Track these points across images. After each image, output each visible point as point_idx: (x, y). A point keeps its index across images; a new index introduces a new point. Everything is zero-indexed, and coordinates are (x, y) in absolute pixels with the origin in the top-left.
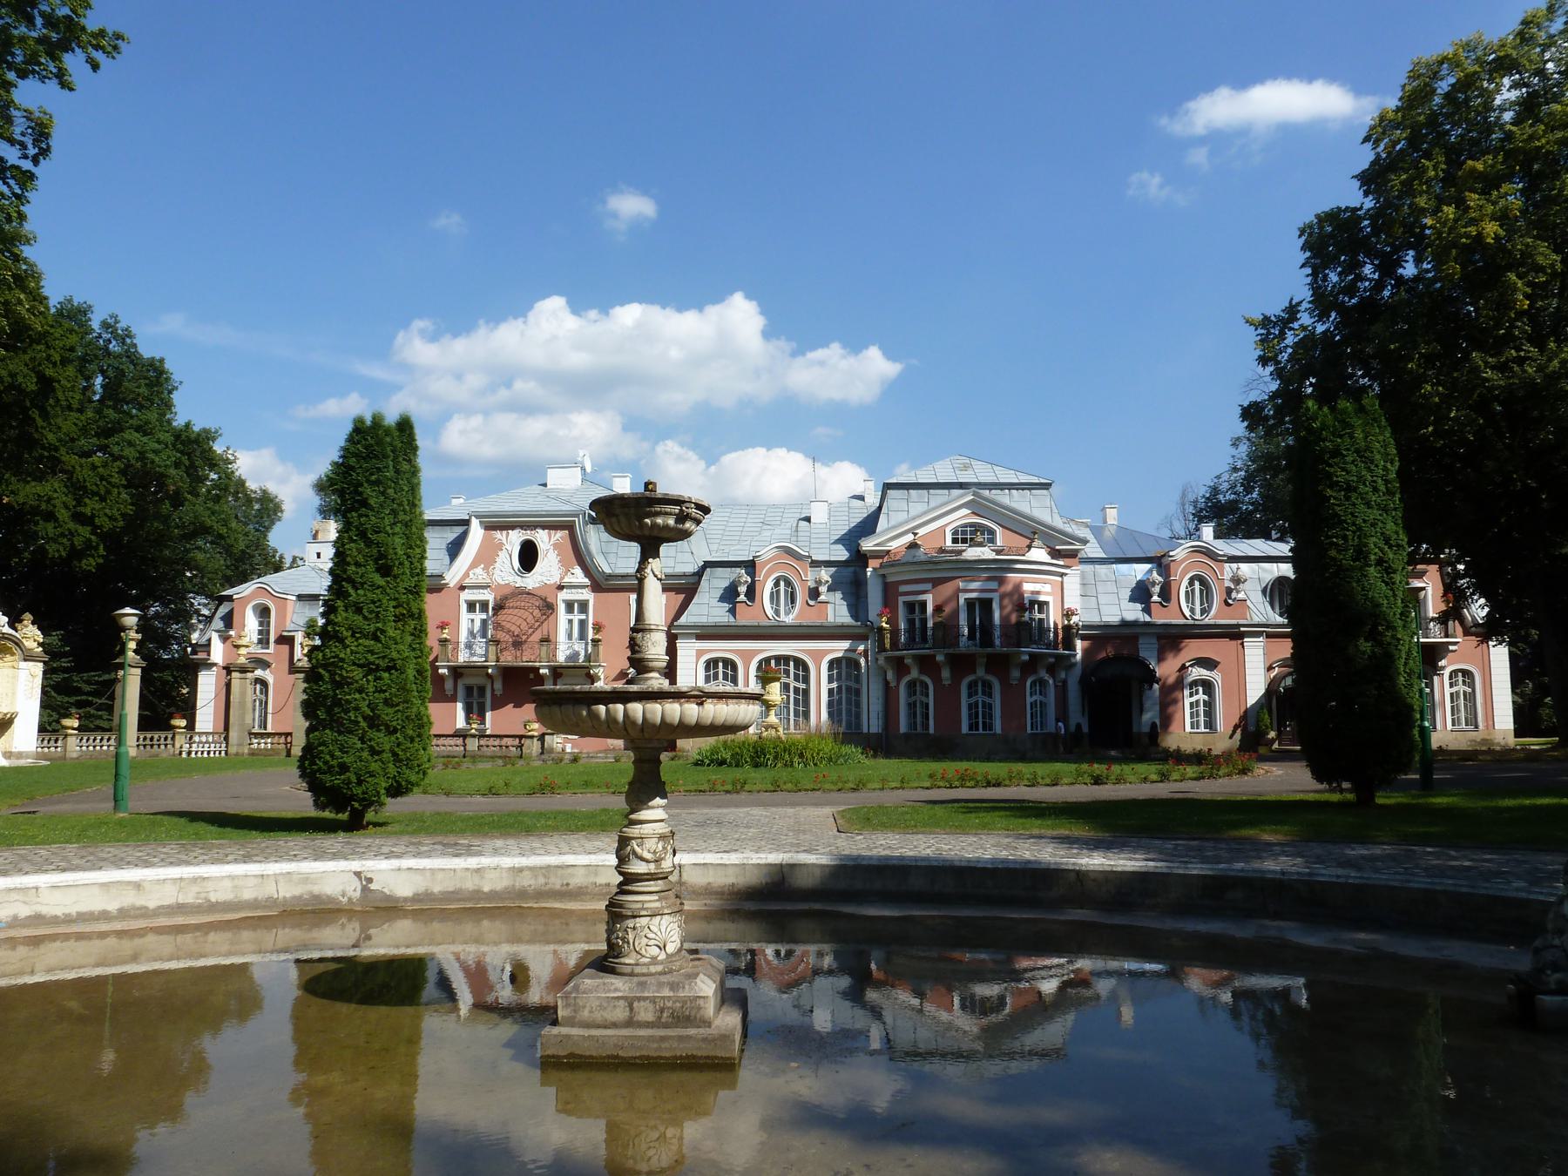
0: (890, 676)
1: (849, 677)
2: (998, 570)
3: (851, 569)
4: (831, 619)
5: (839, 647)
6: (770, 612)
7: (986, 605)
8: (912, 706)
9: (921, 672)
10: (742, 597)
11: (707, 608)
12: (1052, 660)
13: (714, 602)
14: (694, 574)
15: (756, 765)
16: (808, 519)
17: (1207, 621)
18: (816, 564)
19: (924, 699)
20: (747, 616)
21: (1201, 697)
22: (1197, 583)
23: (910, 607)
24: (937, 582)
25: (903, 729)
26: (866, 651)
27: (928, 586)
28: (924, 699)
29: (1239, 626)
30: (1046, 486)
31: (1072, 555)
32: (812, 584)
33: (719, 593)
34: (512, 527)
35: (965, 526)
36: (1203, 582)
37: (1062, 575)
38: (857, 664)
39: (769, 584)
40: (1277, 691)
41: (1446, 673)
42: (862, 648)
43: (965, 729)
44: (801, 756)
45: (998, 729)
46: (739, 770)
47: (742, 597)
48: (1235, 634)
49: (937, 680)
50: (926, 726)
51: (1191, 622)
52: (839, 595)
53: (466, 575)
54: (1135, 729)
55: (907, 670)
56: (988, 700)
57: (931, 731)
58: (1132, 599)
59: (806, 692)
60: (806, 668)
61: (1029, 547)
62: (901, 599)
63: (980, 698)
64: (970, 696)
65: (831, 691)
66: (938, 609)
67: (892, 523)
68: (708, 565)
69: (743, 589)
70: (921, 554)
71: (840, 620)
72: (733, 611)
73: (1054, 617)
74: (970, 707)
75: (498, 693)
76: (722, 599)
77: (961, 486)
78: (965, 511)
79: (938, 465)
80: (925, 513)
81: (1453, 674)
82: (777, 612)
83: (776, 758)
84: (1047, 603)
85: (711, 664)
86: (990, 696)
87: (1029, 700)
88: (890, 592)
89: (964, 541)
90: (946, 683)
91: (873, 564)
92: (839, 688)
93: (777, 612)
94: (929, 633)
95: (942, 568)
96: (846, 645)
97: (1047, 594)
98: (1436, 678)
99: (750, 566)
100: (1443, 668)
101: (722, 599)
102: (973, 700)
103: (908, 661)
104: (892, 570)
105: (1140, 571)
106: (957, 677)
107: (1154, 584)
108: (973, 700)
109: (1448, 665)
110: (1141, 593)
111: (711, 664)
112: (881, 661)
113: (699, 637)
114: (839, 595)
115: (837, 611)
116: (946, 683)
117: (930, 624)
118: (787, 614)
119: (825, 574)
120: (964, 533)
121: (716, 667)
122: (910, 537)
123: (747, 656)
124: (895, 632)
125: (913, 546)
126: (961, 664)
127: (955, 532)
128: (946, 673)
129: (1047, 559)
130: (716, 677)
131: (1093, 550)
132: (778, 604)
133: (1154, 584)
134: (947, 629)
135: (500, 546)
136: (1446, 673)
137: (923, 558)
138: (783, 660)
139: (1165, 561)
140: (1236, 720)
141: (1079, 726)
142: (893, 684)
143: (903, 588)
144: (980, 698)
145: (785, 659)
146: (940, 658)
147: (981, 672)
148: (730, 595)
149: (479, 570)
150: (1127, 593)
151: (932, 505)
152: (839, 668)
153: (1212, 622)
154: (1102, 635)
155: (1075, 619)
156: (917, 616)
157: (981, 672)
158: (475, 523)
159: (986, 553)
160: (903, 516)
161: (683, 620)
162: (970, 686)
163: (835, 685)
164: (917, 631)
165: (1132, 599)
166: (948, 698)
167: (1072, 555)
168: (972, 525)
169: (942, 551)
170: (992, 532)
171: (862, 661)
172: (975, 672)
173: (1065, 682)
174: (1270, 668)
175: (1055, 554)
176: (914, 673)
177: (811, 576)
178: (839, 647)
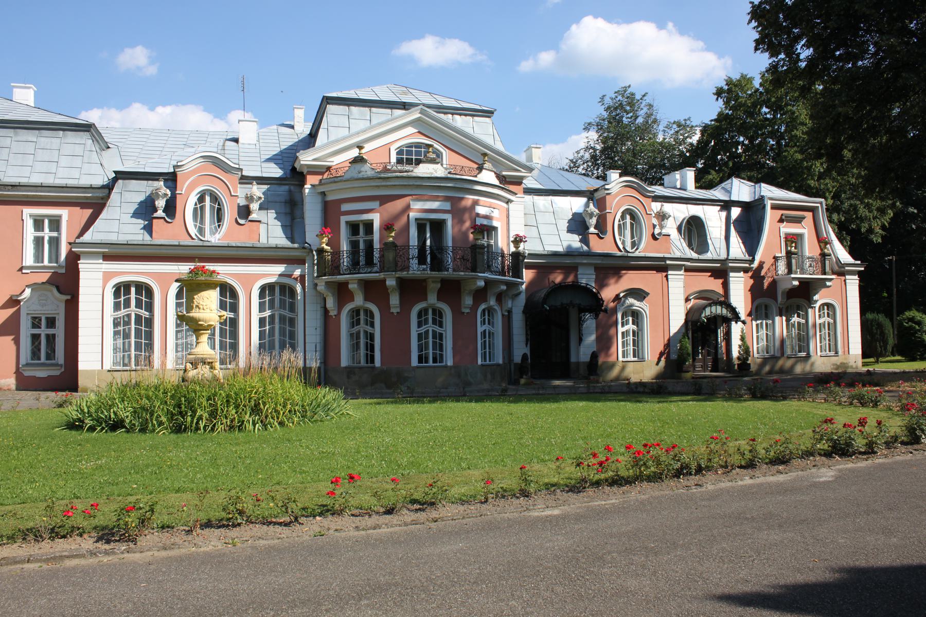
0: (331, 303)
1: (282, 303)
2: (456, 189)
3: (287, 188)
4: (263, 241)
5: (272, 272)
6: (193, 231)
7: (438, 227)
8: (355, 337)
9: (366, 299)
10: (160, 213)
11: (118, 223)
12: (504, 287)
13: (127, 218)
14: (103, 187)
15: (179, 429)
16: (236, 140)
17: (637, 254)
18: (246, 180)
19: (369, 329)
20: (166, 234)
21: (631, 327)
22: (628, 217)
23: (354, 228)
24: (384, 200)
25: (344, 363)
26: (302, 278)
27: (375, 205)
28: (369, 329)
29: (664, 259)
30: (488, 113)
31: (518, 181)
32: (242, 202)
33: (133, 208)
35: (410, 146)
36: (633, 217)
37: (508, 201)
38: (292, 292)
39: (193, 199)
40: (699, 320)
41: (817, 305)
42: (297, 272)
44: (256, 410)
45: (450, 363)
46: (142, 437)
47: (160, 213)
48: (661, 266)
49: (384, 306)
50: (371, 359)
51: (623, 253)
52: (272, 214)
54: (573, 359)
55: (350, 297)
56: (438, 329)
57: (378, 363)
58: (570, 230)
60: (234, 294)
61: (480, 168)
62: (344, 219)
63: (430, 327)
64: (420, 325)
65: (262, 322)
66: (387, 227)
67: (332, 138)
68: (120, 175)
69: (161, 203)
70: (367, 170)
71: (273, 242)
72: (149, 229)
73: (503, 243)
74: (420, 336)
76: (136, 215)
77: (405, 106)
78: (411, 130)
79: (376, 89)
80: (364, 131)
81: (823, 305)
82: (201, 231)
83: (213, 414)
84: (495, 229)
85: (122, 289)
87: (480, 329)
88: (330, 212)
89: (409, 162)
90: (395, 310)
91: (312, 180)
92: (272, 317)
93: (201, 231)
94: (376, 254)
95: (389, 186)
96: (280, 269)
97: (498, 220)
98: (810, 310)
99: (171, 179)
100: (816, 301)
101: (136, 215)
102: (423, 329)
103: (352, 286)
104: (334, 187)
105: (578, 204)
106: (406, 304)
107: (591, 215)
108: (423, 329)
109: (820, 298)
110: (578, 224)
111: (122, 289)
112: (321, 287)
113: (107, 257)
114: (272, 214)
115: (270, 231)
116: (393, 310)
117: (377, 245)
118: (213, 233)
119: (258, 191)
120: (409, 153)
121: (127, 292)
122: (355, 153)
124: (336, 253)
125: (359, 160)
126: (412, 289)
127: (400, 152)
128: (394, 300)
129: (497, 182)
130: (127, 304)
131: (530, 183)
132: (202, 221)
133: (591, 215)
134: (395, 253)
136: (817, 305)
137: (370, 173)
139: (597, 195)
140: (661, 348)
141: (524, 356)
142: (333, 313)
143: (345, 207)
146: (391, 282)
147: (432, 299)
148: (146, 210)
150: (564, 225)
151: (374, 122)
152: (272, 292)
153: (642, 254)
154: (549, 263)
155: (522, 246)
156: (361, 238)
157: (432, 299)
159: (437, 170)
160: (345, 132)
161: (87, 237)
162: (419, 315)
163: (267, 313)
164: (362, 255)
165: (570, 230)
166: (396, 329)
167: (518, 181)
168: (418, 145)
169: (386, 170)
170: (439, 155)
171: (299, 288)
172: (426, 299)
173: (510, 312)
174: (687, 300)
175: (502, 179)
176: (359, 300)
177: (241, 192)
178: (272, 272)
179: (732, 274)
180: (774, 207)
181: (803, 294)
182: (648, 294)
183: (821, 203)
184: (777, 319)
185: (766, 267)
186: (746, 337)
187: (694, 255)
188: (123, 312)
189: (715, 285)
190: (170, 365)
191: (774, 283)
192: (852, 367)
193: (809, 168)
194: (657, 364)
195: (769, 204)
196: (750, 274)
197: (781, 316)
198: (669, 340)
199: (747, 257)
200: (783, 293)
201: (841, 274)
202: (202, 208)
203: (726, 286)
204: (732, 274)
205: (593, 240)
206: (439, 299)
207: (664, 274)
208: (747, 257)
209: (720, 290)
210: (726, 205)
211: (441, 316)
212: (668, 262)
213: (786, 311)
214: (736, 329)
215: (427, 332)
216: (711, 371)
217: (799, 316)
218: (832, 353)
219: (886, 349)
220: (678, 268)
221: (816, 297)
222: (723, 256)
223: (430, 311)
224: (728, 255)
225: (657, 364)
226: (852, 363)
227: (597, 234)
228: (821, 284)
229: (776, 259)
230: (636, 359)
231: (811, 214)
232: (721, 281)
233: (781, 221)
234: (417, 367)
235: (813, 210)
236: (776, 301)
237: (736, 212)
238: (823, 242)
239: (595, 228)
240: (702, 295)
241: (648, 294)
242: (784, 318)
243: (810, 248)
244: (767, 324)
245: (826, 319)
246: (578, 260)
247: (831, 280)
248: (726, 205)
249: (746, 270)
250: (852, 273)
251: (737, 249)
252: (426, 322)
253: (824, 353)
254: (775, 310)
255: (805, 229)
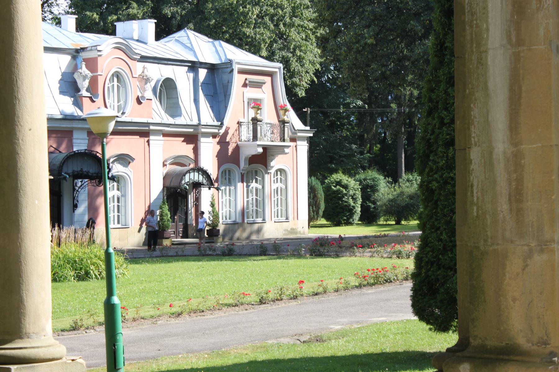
22: (115, 79)
29: (148, 124)
48: (143, 132)
109: (276, 163)
136: (272, 171)
140: (142, 215)
179: (203, 140)
180: (241, 72)
181: (262, 160)
182: (133, 159)
183: (279, 68)
184: (240, 185)
185: (231, 132)
186: (216, 204)
187: (171, 121)
189: (187, 150)
191: (237, 148)
192: (300, 233)
193: (245, 15)
194: (139, 231)
195: (236, 68)
196: (217, 140)
197: (242, 182)
198: (149, 207)
199: (217, 123)
200: (245, 159)
201: (293, 140)
203: (196, 151)
204: (203, 140)
205: (86, 102)
207: (146, 139)
208: (217, 123)
209: (192, 156)
210: (193, 66)
212: (152, 127)
213: (246, 178)
214: (206, 194)
216: (182, 237)
217: (256, 182)
218: (284, 219)
219: (318, 213)
220: (157, 133)
221: (272, 164)
222: (195, 122)
224: (199, 120)
225: (139, 231)
226: (300, 229)
227: (91, 98)
228: (281, 150)
229: (239, 124)
230: (119, 226)
231: (270, 78)
232: (192, 146)
233: (245, 85)
235: (270, 74)
236: (239, 166)
237: (203, 73)
238: (278, 108)
239: (87, 90)
240: (178, 161)
241: (133, 159)
242: (245, 184)
243: (268, 115)
244: (230, 190)
245: (280, 185)
246: (75, 125)
247: (289, 147)
248: (193, 66)
249: (214, 136)
250: (302, 139)
251: (208, 116)
253: (276, 219)
254: (237, 176)
255: (264, 94)
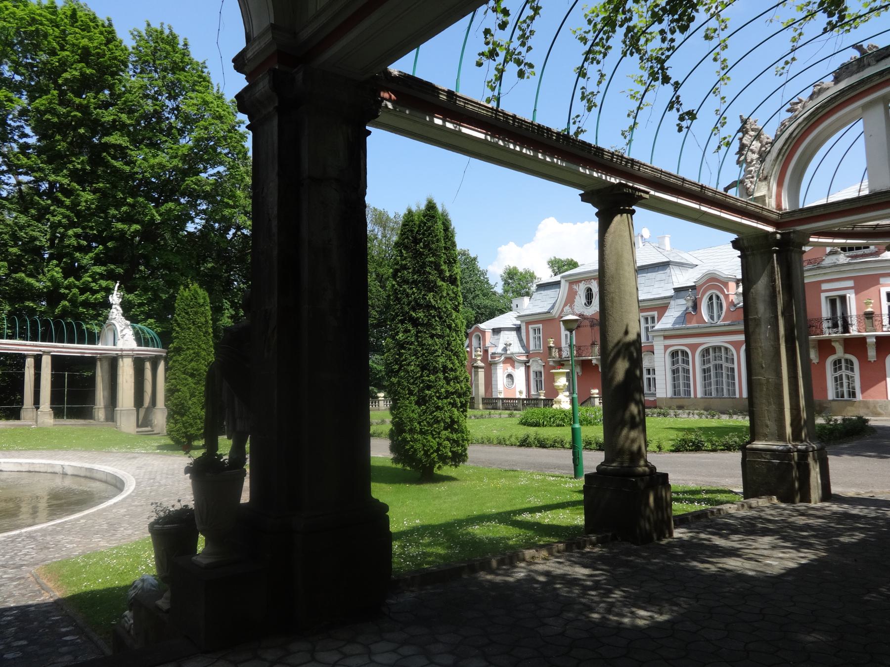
6: (706, 318)
10: (690, 309)
34: (580, 281)
43: (831, 395)
53: (562, 310)
56: (850, 373)
59: (733, 369)
63: (844, 372)
64: (835, 371)
74: (836, 378)
75: (580, 374)
82: (712, 317)
85: (674, 354)
86: (852, 370)
106: (823, 357)
108: (838, 374)
113: (666, 337)
123: (694, 347)
132: (712, 312)
135: (576, 293)
138: (717, 349)
144: (844, 372)
145: (720, 348)
149: (567, 307)
157: (840, 353)
158: (563, 282)
188: (675, 367)
190: (699, 395)
202: (712, 304)
206: (846, 352)
211: (852, 363)
215: (841, 376)
223: (843, 361)
234: (833, 400)
252: (840, 368)
